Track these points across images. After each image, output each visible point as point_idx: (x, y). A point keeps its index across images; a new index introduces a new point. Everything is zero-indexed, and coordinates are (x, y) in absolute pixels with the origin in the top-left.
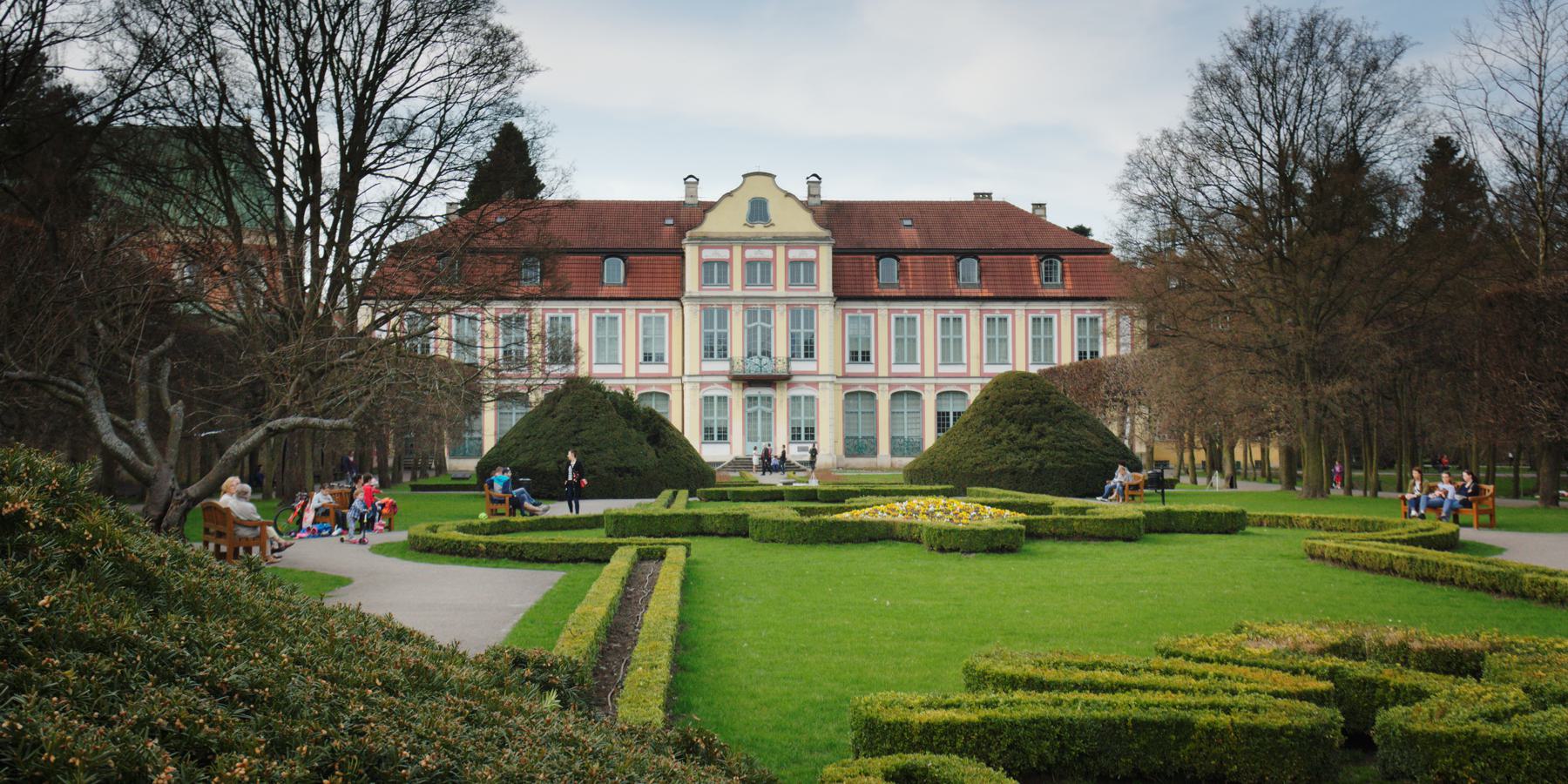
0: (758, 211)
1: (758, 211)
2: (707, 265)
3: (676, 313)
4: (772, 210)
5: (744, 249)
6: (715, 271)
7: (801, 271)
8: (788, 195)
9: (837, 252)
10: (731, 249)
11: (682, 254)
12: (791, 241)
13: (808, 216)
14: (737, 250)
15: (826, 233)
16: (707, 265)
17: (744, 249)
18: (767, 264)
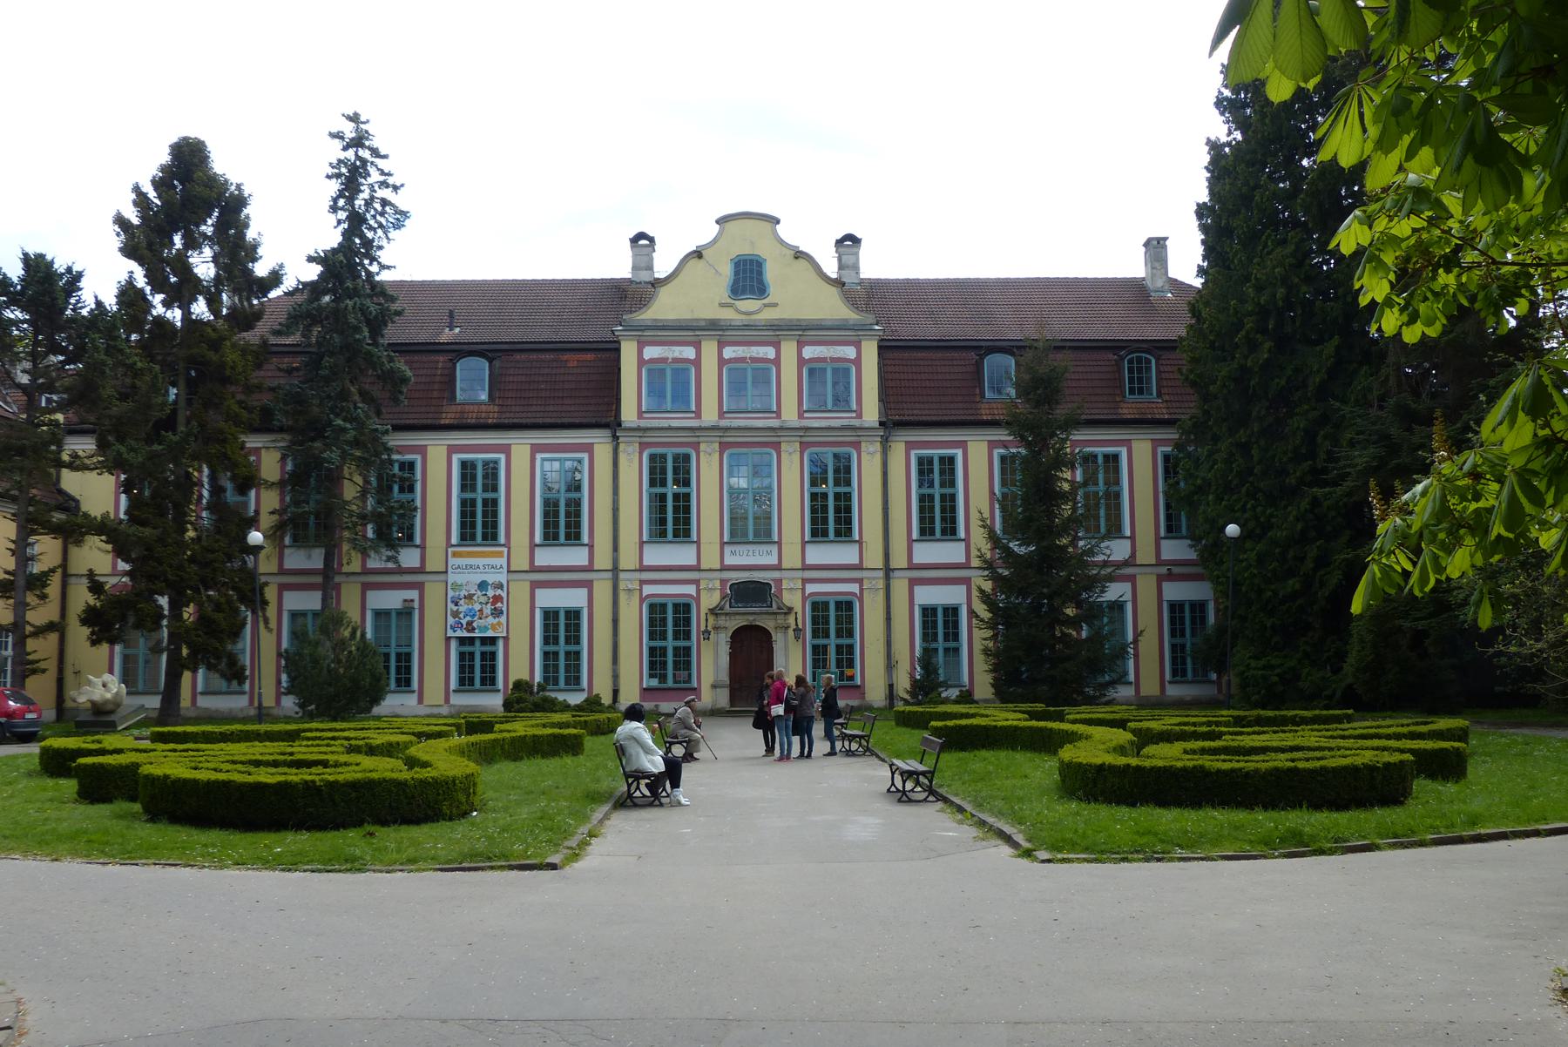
0: (749, 277)
1: (749, 277)
2: (654, 371)
3: (603, 451)
4: (771, 274)
5: (721, 345)
6: (673, 385)
7: (828, 383)
8: (799, 255)
9: (882, 349)
10: (697, 346)
11: (618, 350)
12: (803, 331)
13: (834, 291)
14: (709, 349)
15: (870, 318)
16: (654, 371)
17: (721, 345)
18: (764, 373)
